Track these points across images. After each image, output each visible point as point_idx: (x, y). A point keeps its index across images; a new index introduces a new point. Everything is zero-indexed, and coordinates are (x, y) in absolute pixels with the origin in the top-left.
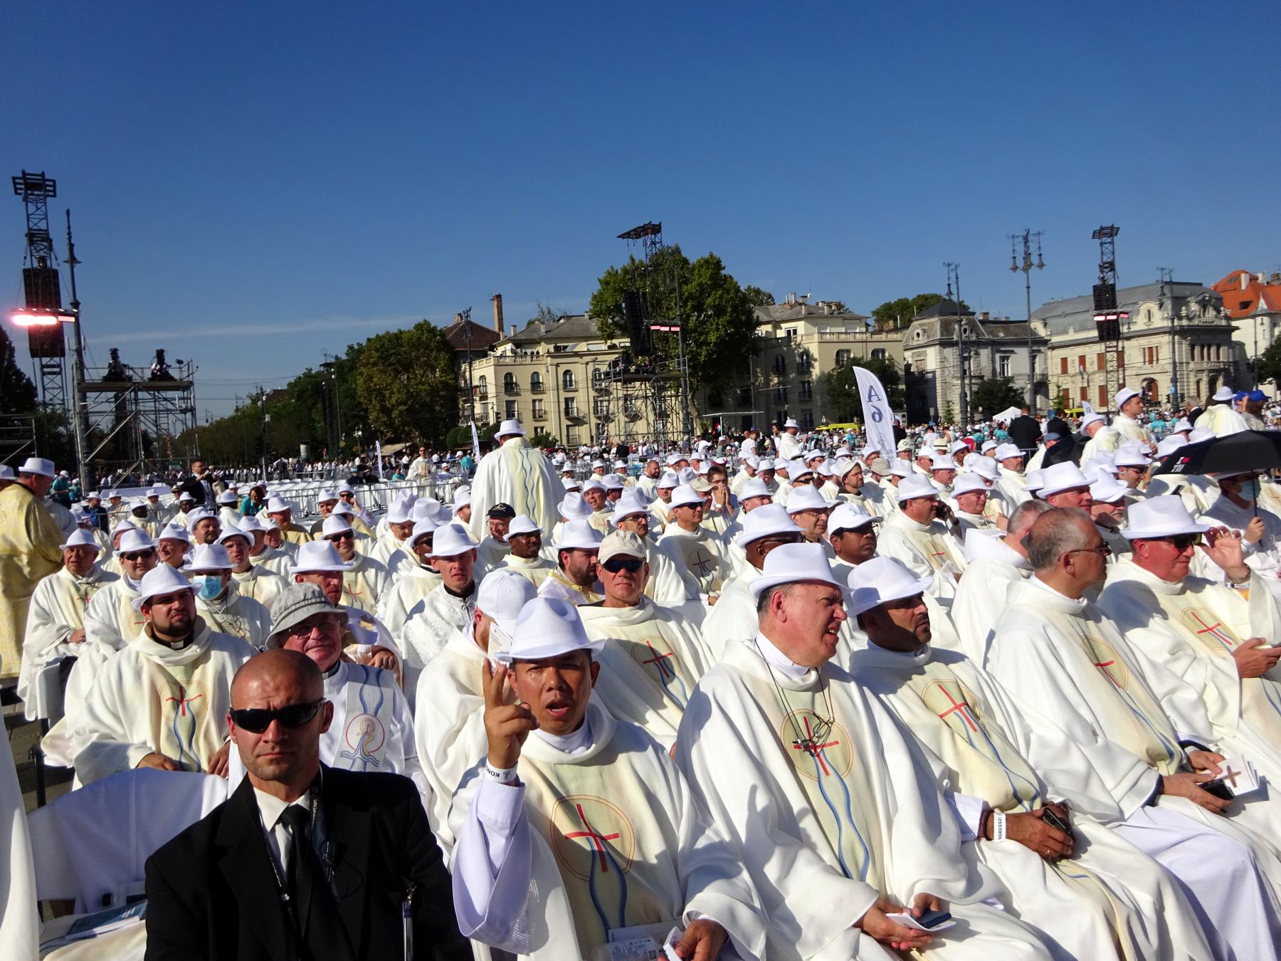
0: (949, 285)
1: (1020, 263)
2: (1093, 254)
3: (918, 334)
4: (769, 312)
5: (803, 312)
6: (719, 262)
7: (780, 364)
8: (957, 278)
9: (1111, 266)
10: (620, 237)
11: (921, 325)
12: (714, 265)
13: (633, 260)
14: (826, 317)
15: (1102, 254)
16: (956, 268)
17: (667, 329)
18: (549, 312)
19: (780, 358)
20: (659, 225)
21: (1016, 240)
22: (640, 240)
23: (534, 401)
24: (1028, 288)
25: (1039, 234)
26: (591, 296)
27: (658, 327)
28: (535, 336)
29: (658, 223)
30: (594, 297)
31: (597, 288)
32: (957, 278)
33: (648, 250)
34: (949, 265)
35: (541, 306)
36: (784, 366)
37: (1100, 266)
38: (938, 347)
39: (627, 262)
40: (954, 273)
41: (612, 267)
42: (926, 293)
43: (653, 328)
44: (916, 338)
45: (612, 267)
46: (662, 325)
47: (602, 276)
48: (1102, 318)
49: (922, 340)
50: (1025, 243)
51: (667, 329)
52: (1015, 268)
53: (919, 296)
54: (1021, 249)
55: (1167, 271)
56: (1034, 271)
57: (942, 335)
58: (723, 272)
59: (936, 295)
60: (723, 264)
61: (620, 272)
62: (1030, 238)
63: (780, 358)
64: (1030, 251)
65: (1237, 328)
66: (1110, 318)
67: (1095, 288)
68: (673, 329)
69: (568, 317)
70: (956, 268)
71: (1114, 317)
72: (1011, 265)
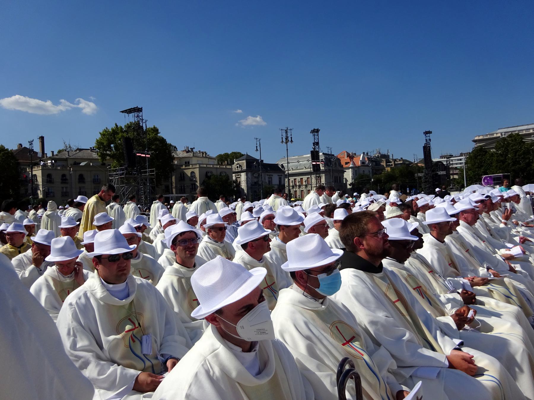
0: (257, 147)
1: (284, 140)
2: (311, 139)
3: (237, 167)
4: (177, 154)
5: (192, 155)
6: (158, 130)
7: (182, 176)
8: (260, 144)
9: (317, 144)
10: (122, 112)
11: (238, 164)
12: (155, 130)
13: (116, 125)
14: (201, 157)
15: (315, 139)
16: (260, 140)
17: (144, 155)
18: (70, 147)
19: (182, 173)
20: (142, 108)
21: (283, 131)
22: (131, 115)
23: (63, 188)
24: (287, 150)
25: (291, 129)
26: (96, 140)
27: (140, 154)
28: (64, 157)
29: (141, 107)
30: (97, 141)
31: (99, 137)
32: (260, 144)
33: (136, 119)
34: (257, 139)
35: (66, 144)
36: (184, 176)
37: (313, 143)
38: (245, 173)
39: (114, 126)
40: (259, 142)
41: (107, 128)
42: (236, 151)
43: (138, 154)
44: (237, 169)
45: (107, 128)
46: (142, 154)
47: (101, 132)
48: (315, 163)
49: (240, 170)
50: (286, 133)
51: (144, 155)
52: (283, 142)
53: (233, 153)
54: (284, 134)
55: (330, 148)
56: (289, 143)
57: (246, 168)
58: (159, 135)
59: (239, 153)
60: (159, 131)
61: (110, 130)
62: (288, 131)
63: (182, 173)
64: (288, 136)
65: (346, 171)
66: (317, 163)
67: (312, 152)
68: (147, 156)
69: (80, 150)
70: (260, 140)
71: (319, 163)
72: (281, 141)
